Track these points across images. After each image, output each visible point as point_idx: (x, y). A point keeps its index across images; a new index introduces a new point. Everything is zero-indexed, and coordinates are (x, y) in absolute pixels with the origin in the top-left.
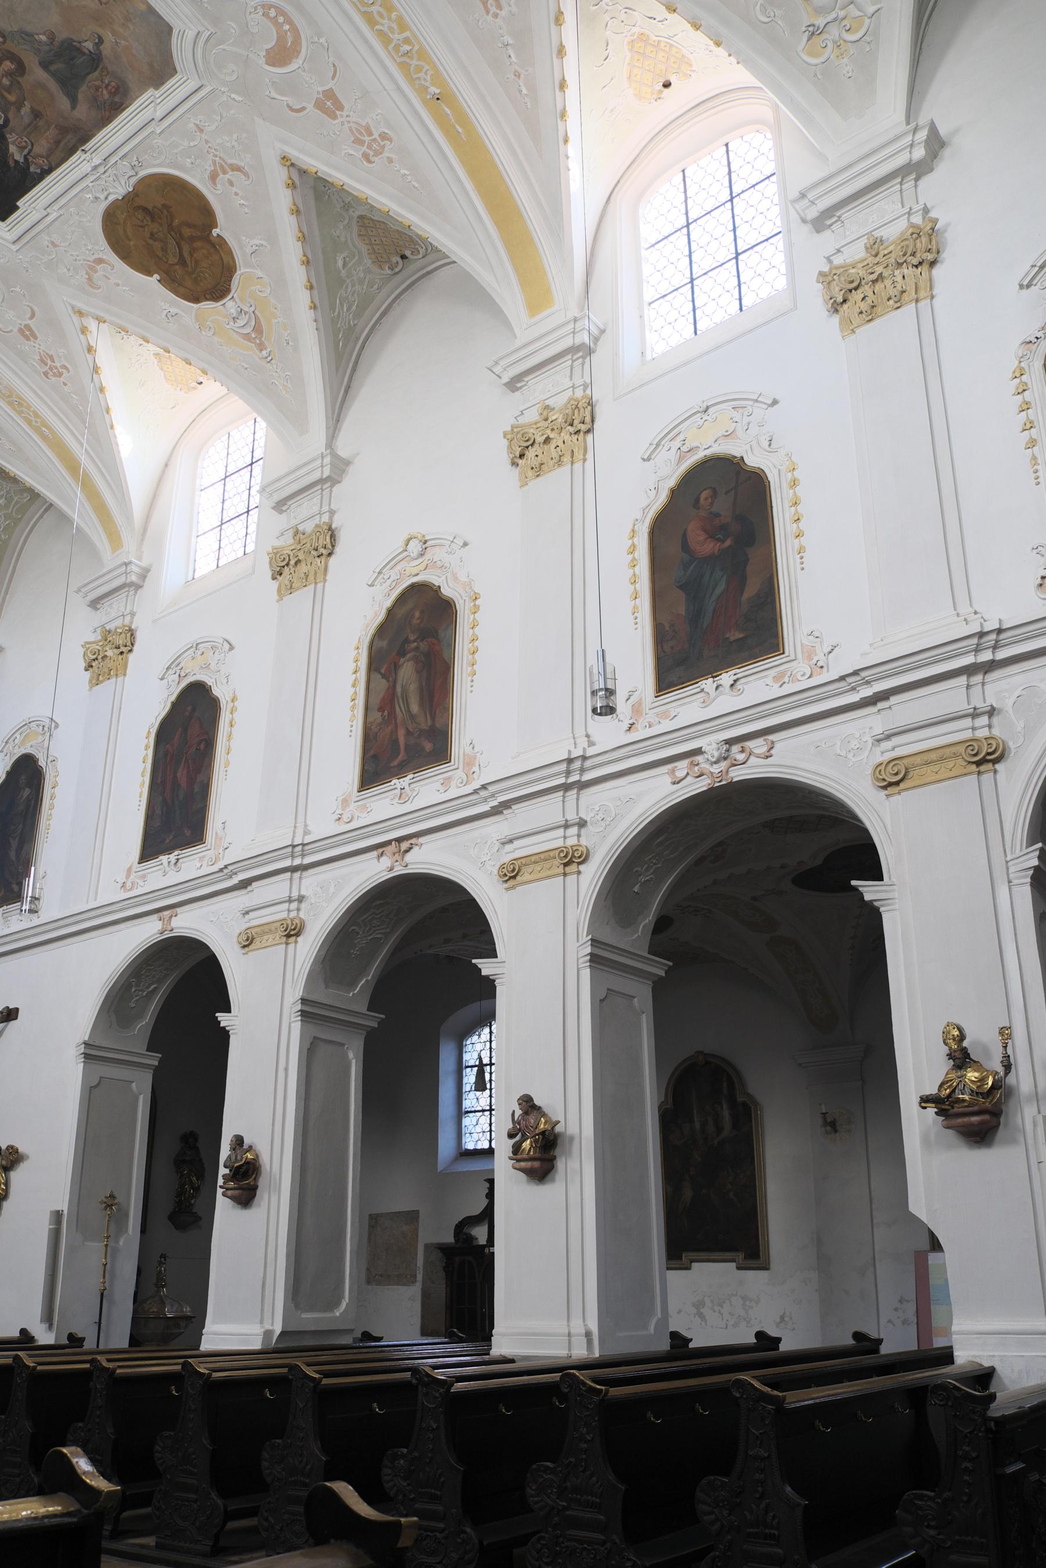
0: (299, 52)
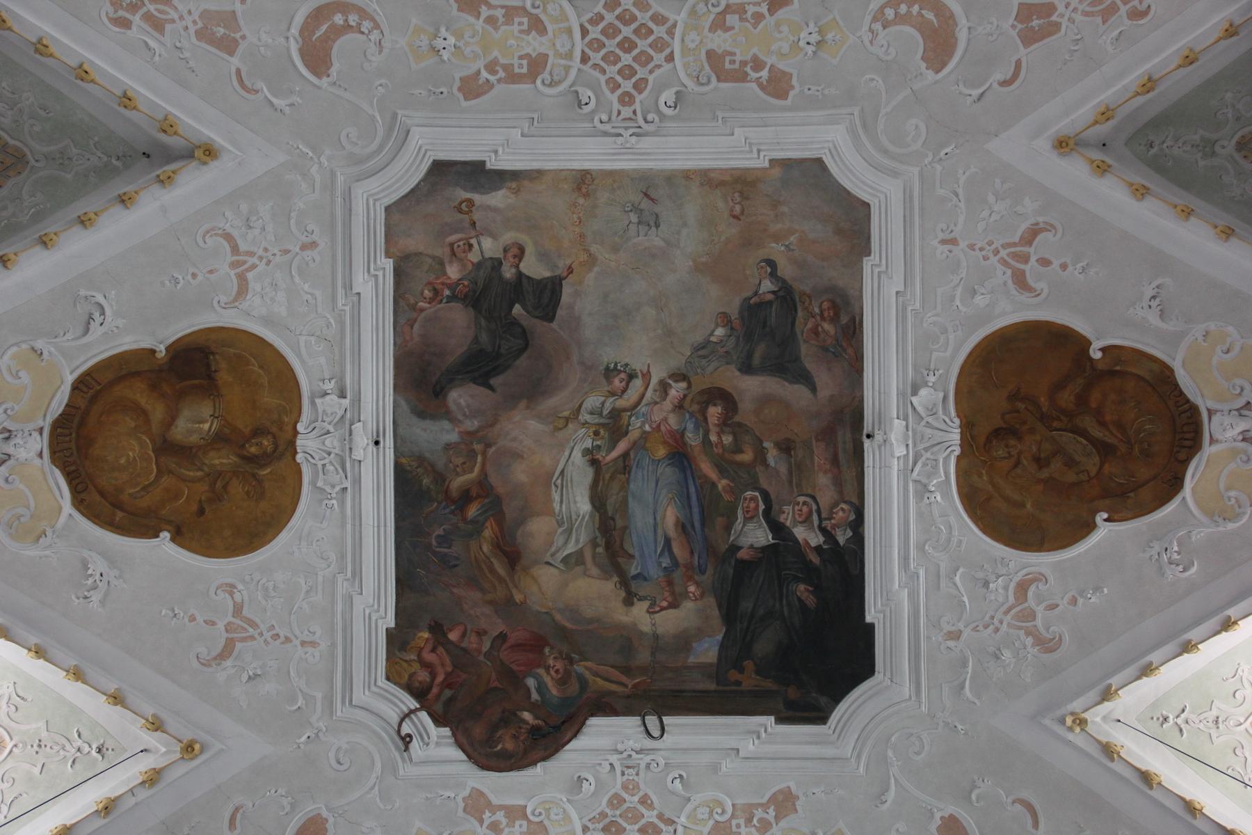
0: (952, 16)
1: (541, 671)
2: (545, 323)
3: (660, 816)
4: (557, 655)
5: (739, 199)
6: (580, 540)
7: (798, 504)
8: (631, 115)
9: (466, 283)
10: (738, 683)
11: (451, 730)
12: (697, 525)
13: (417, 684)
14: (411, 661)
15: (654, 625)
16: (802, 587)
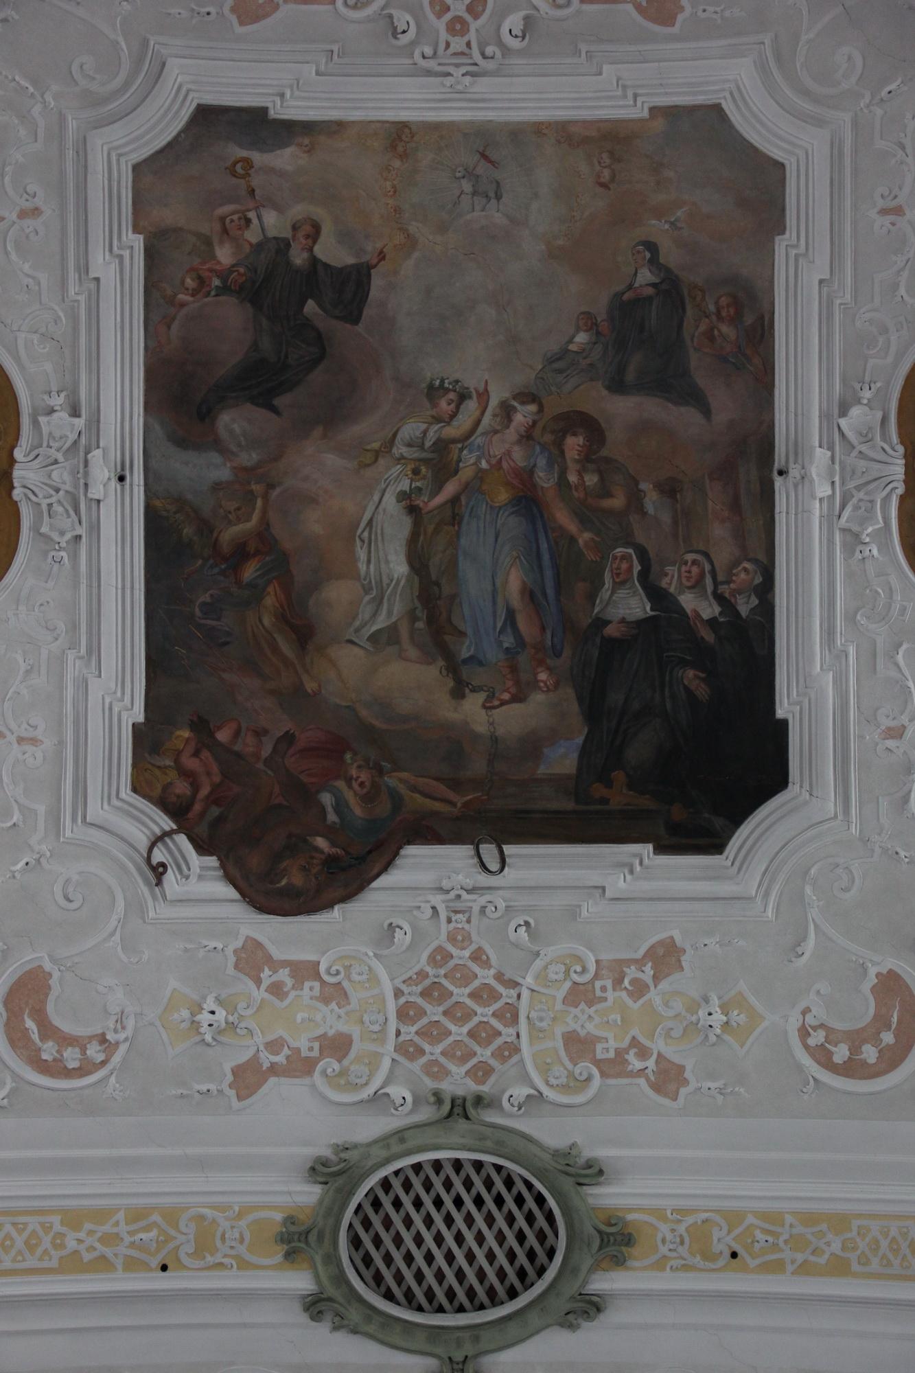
1: (341, 784)
2: (348, 326)
3: (499, 977)
4: (362, 763)
5: (608, 161)
6: (392, 612)
7: (686, 563)
8: (464, 48)
9: (242, 270)
10: (604, 801)
11: (220, 859)
12: (550, 592)
13: (174, 799)
14: (166, 767)
15: (492, 724)
16: (691, 673)
